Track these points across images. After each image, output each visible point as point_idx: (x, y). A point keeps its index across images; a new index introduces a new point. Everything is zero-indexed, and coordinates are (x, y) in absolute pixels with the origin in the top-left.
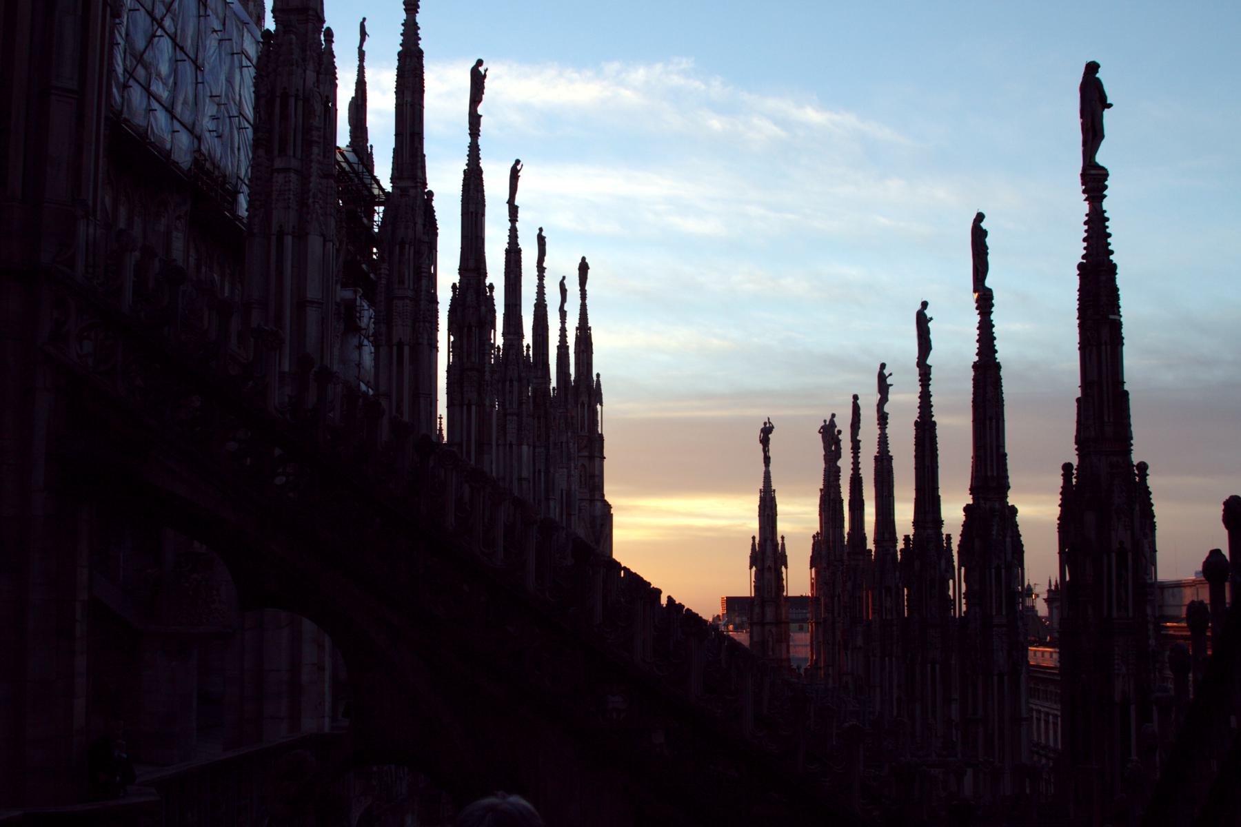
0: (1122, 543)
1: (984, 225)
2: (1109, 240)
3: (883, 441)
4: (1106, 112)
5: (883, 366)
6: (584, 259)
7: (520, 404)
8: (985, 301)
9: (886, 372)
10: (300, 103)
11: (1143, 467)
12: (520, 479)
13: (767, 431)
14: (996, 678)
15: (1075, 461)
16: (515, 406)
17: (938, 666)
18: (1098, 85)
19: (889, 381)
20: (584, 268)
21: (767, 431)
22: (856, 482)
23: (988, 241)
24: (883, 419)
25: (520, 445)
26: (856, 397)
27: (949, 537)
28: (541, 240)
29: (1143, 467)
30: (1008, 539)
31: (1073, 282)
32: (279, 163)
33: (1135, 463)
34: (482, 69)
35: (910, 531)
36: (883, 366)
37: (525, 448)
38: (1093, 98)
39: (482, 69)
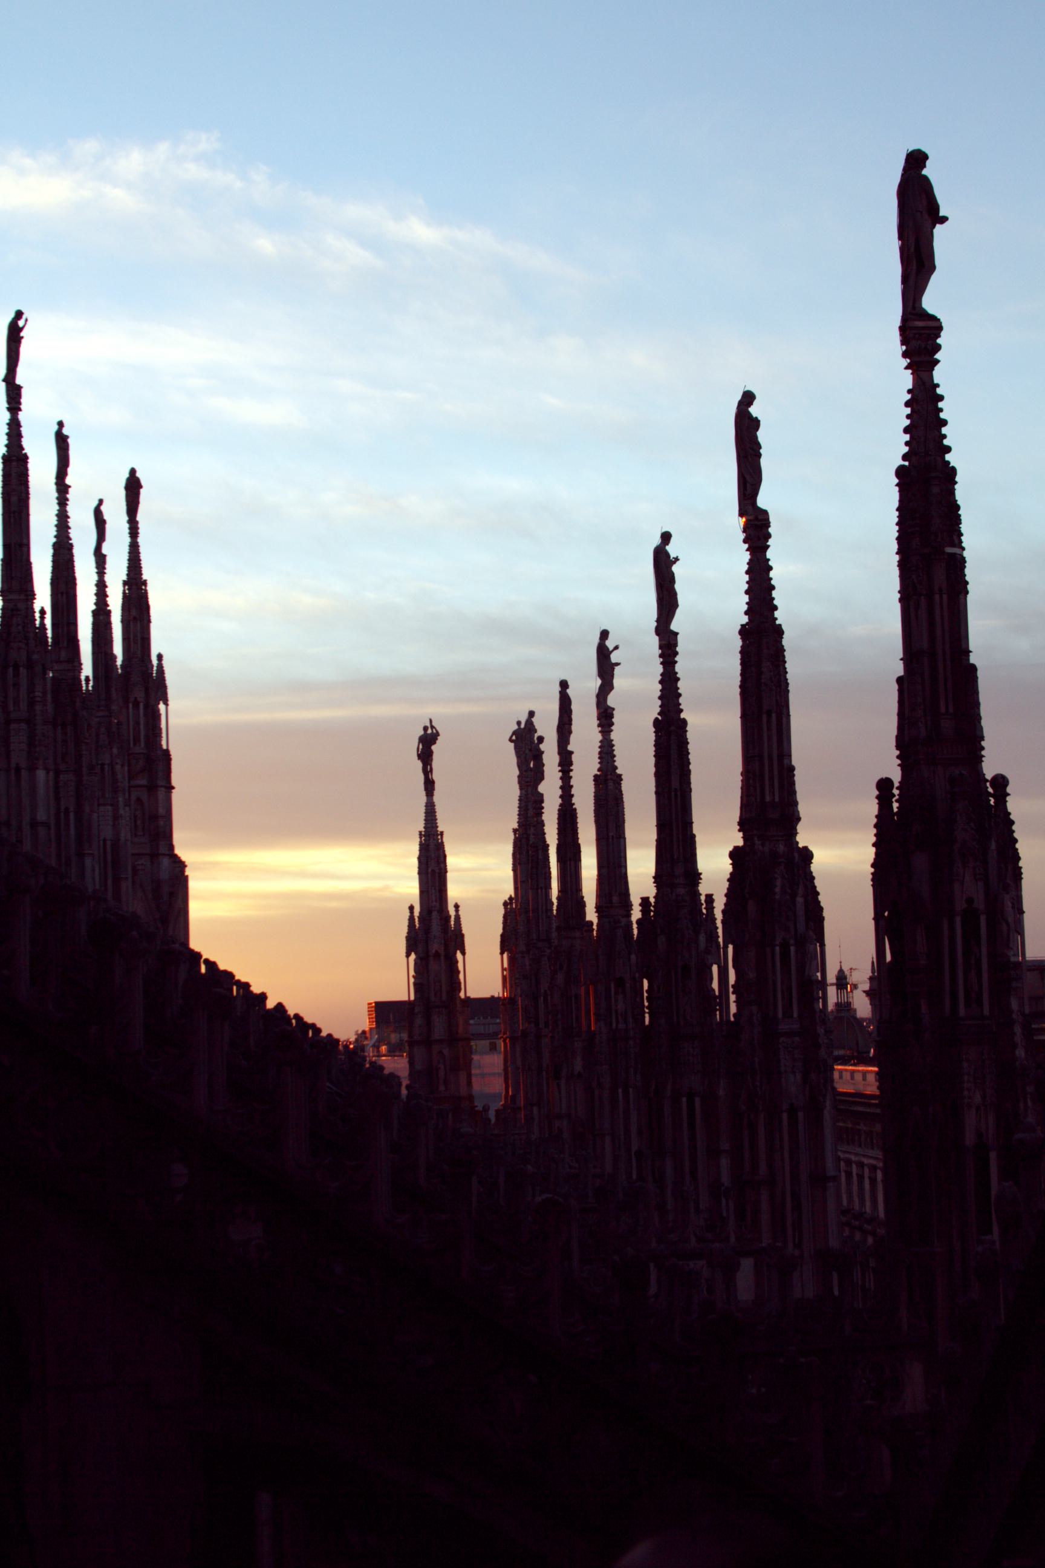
0: (970, 901)
1: (754, 410)
2: (944, 430)
3: (607, 752)
4: (939, 230)
5: (604, 635)
6: (133, 472)
7: (32, 703)
8: (757, 530)
9: (610, 644)
11: (1000, 782)
12: (34, 824)
13: (428, 740)
14: (785, 1116)
15: (896, 776)
16: (23, 706)
17: (697, 1100)
18: (926, 187)
19: (614, 657)
20: (133, 486)
21: (428, 740)
23: (762, 435)
24: (606, 717)
25: (32, 769)
26: (564, 685)
27: (710, 898)
28: (62, 442)
29: (1000, 782)
30: (800, 900)
33: (989, 777)
35: (651, 891)
36: (604, 635)
37: (41, 774)
38: (918, 209)
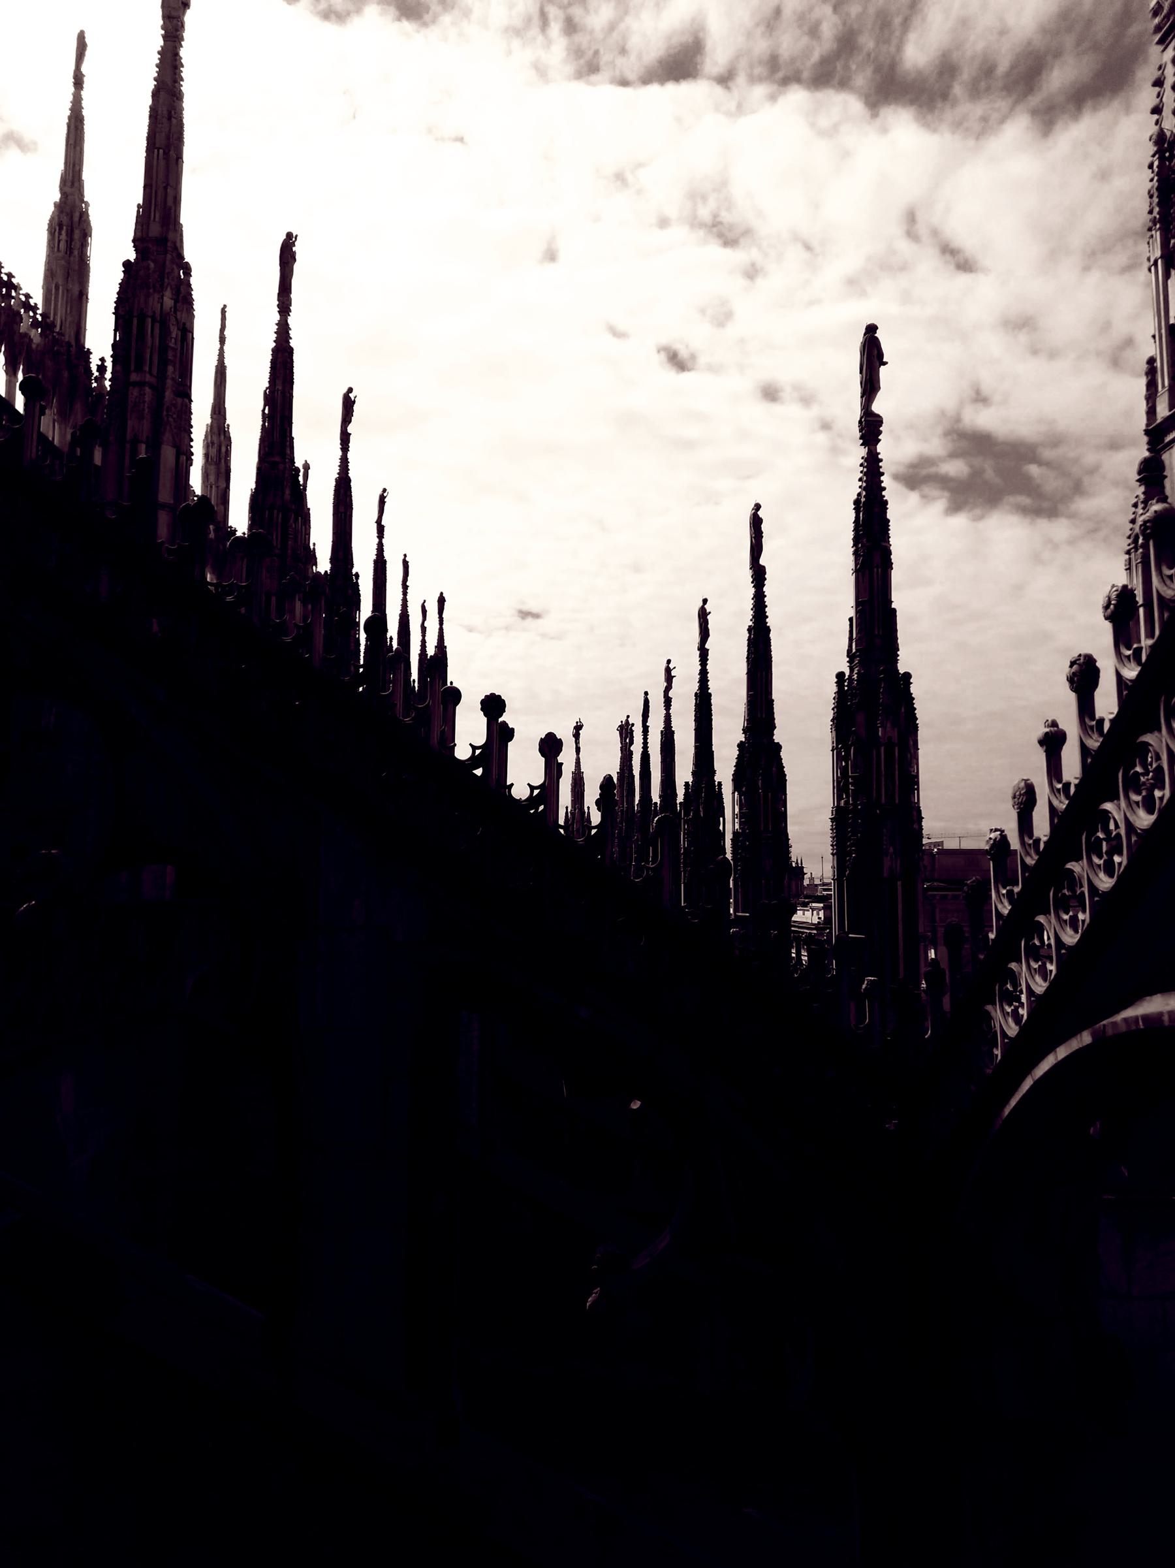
2: (882, 478)
5: (669, 662)
9: (671, 666)
10: (157, 325)
11: (908, 676)
20: (441, 601)
22: (645, 757)
24: (668, 702)
26: (646, 693)
28: (406, 564)
31: (849, 516)
32: (134, 377)
34: (352, 395)
36: (669, 662)
39: (352, 395)
